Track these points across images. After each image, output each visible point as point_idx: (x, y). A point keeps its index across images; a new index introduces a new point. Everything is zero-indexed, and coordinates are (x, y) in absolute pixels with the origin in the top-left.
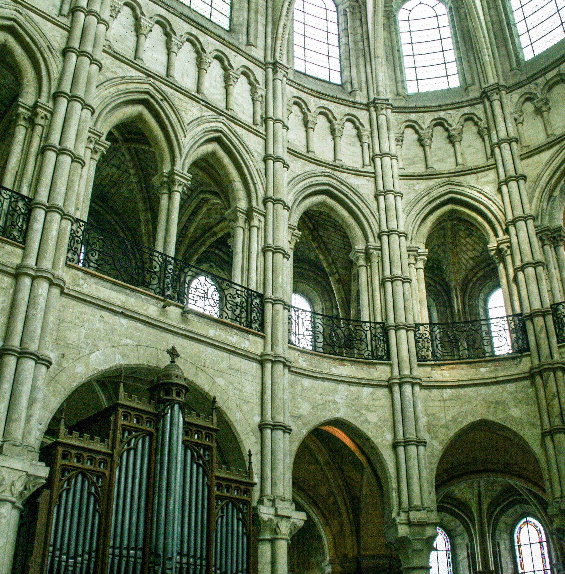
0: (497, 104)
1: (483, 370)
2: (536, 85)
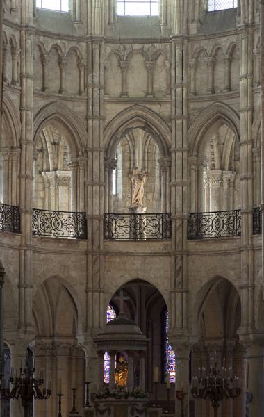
0: (97, 51)
1: (61, 245)
2: (124, 47)
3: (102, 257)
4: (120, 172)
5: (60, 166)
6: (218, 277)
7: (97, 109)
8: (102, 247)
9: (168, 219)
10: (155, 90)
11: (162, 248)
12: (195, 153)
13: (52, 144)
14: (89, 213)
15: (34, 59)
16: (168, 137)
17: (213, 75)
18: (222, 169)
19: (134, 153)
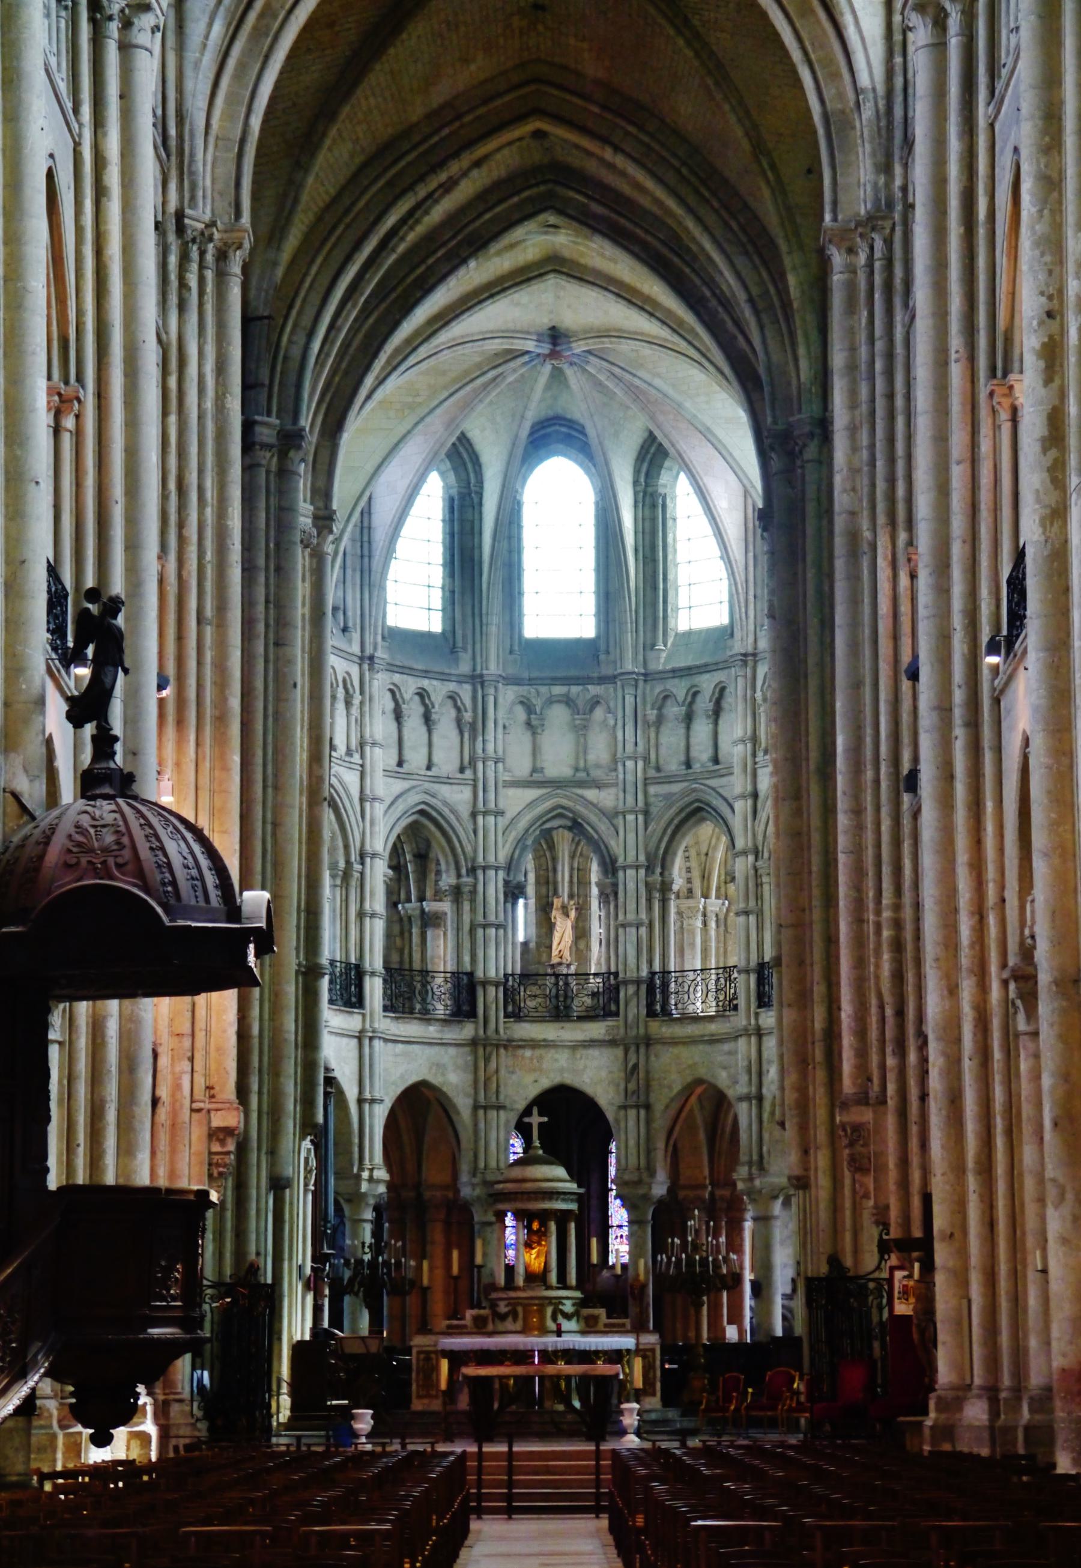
0: (491, 699)
1: (431, 1028)
2: (538, 692)
3: (502, 1051)
4: (532, 902)
5: (429, 893)
6: (699, 1081)
7: (491, 796)
8: (502, 1031)
9: (612, 981)
10: (590, 763)
11: (603, 1031)
12: (658, 870)
13: (415, 856)
14: (480, 974)
15: (384, 713)
16: (612, 843)
17: (688, 738)
18: (706, 896)
19: (555, 870)
